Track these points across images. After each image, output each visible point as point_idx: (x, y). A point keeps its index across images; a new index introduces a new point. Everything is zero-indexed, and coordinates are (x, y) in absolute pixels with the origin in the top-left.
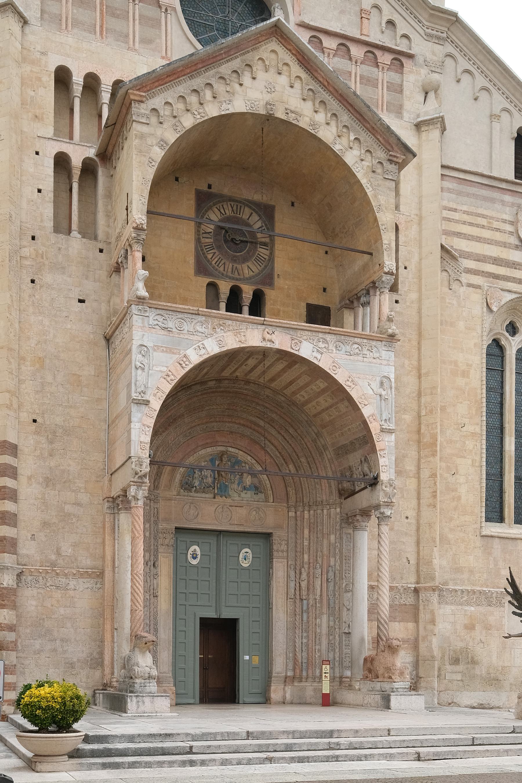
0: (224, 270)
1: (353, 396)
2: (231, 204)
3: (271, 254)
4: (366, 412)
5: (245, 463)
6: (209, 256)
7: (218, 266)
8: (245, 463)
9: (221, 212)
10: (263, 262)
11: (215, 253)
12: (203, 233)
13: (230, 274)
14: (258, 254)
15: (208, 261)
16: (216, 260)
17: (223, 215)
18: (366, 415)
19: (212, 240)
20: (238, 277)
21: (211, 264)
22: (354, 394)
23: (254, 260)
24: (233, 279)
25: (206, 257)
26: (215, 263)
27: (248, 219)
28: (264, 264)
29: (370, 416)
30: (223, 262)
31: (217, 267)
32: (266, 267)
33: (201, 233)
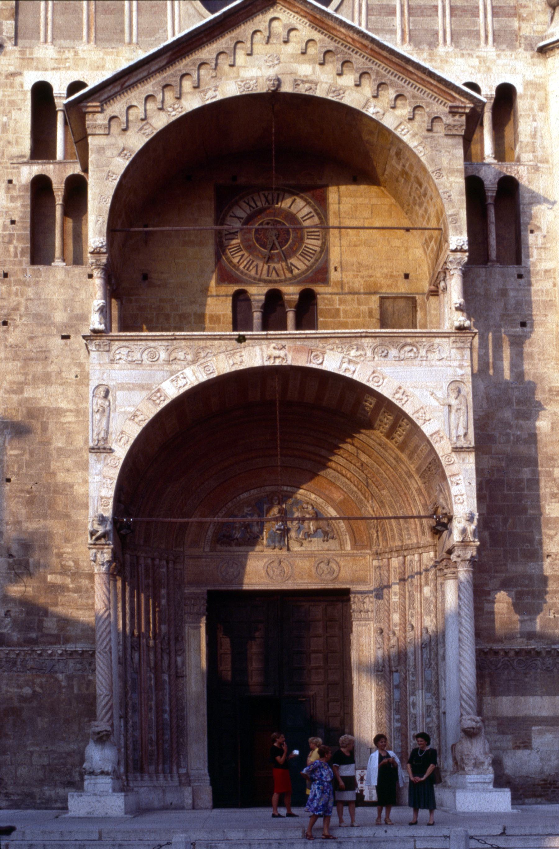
0: (257, 273)
1: (407, 411)
2: (264, 195)
3: (324, 244)
4: (427, 429)
5: (308, 503)
6: (235, 261)
7: (247, 270)
8: (308, 503)
9: (250, 206)
10: (312, 256)
11: (243, 256)
12: (226, 235)
13: (264, 277)
14: (305, 247)
15: (234, 266)
16: (245, 263)
17: (253, 208)
18: (428, 434)
19: (239, 241)
20: (278, 278)
21: (238, 269)
22: (408, 409)
23: (300, 255)
24: (270, 282)
25: (231, 262)
26: (244, 267)
27: (290, 207)
28: (314, 257)
29: (435, 433)
30: (255, 263)
31: (246, 272)
32: (317, 260)
33: (223, 234)
